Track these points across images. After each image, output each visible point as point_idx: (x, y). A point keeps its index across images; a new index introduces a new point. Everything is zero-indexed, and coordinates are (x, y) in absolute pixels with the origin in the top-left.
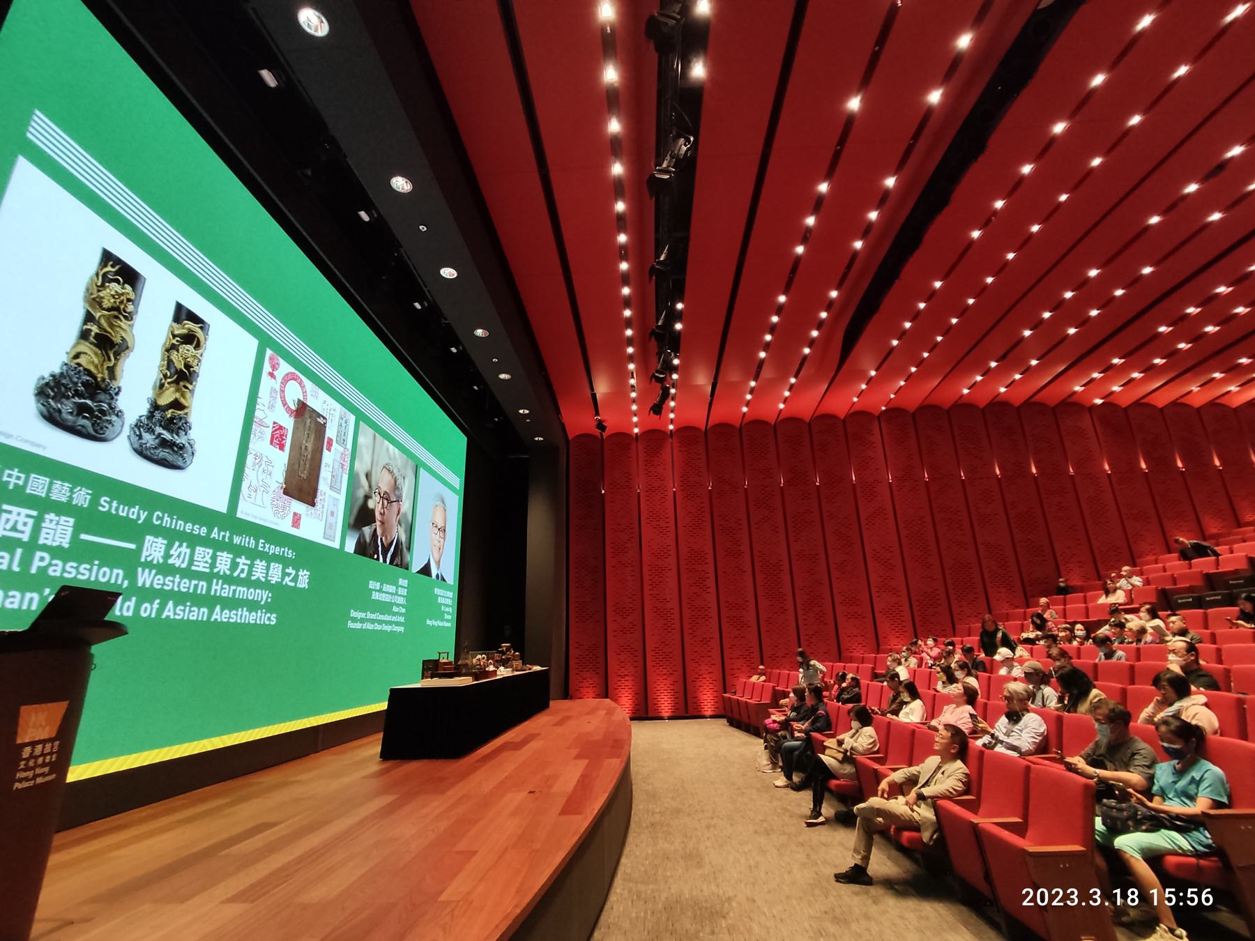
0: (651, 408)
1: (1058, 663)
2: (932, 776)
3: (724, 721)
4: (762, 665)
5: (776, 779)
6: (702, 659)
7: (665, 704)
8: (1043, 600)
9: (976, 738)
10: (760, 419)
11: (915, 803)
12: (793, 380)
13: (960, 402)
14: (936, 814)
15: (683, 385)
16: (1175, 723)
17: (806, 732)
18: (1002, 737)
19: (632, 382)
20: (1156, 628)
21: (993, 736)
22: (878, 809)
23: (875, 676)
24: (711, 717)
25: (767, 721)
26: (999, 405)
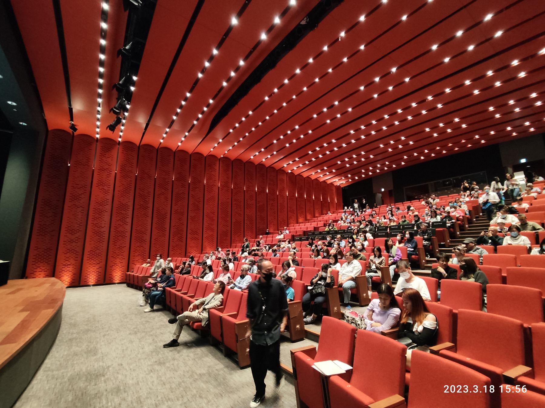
0: (108, 126)
1: (260, 258)
2: (210, 301)
3: (125, 285)
4: (149, 259)
5: (146, 309)
6: (118, 256)
7: (92, 278)
8: (261, 236)
9: (229, 285)
10: (168, 147)
11: (202, 312)
12: (187, 134)
13: (249, 161)
14: (209, 315)
15: (132, 119)
16: (286, 277)
17: (164, 288)
18: (237, 284)
19: (99, 109)
20: (288, 247)
21: (234, 284)
22: (187, 316)
23: (198, 263)
24: (118, 283)
25: (146, 284)
26: (261, 165)
